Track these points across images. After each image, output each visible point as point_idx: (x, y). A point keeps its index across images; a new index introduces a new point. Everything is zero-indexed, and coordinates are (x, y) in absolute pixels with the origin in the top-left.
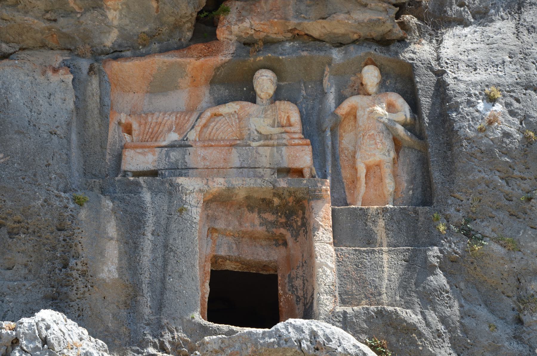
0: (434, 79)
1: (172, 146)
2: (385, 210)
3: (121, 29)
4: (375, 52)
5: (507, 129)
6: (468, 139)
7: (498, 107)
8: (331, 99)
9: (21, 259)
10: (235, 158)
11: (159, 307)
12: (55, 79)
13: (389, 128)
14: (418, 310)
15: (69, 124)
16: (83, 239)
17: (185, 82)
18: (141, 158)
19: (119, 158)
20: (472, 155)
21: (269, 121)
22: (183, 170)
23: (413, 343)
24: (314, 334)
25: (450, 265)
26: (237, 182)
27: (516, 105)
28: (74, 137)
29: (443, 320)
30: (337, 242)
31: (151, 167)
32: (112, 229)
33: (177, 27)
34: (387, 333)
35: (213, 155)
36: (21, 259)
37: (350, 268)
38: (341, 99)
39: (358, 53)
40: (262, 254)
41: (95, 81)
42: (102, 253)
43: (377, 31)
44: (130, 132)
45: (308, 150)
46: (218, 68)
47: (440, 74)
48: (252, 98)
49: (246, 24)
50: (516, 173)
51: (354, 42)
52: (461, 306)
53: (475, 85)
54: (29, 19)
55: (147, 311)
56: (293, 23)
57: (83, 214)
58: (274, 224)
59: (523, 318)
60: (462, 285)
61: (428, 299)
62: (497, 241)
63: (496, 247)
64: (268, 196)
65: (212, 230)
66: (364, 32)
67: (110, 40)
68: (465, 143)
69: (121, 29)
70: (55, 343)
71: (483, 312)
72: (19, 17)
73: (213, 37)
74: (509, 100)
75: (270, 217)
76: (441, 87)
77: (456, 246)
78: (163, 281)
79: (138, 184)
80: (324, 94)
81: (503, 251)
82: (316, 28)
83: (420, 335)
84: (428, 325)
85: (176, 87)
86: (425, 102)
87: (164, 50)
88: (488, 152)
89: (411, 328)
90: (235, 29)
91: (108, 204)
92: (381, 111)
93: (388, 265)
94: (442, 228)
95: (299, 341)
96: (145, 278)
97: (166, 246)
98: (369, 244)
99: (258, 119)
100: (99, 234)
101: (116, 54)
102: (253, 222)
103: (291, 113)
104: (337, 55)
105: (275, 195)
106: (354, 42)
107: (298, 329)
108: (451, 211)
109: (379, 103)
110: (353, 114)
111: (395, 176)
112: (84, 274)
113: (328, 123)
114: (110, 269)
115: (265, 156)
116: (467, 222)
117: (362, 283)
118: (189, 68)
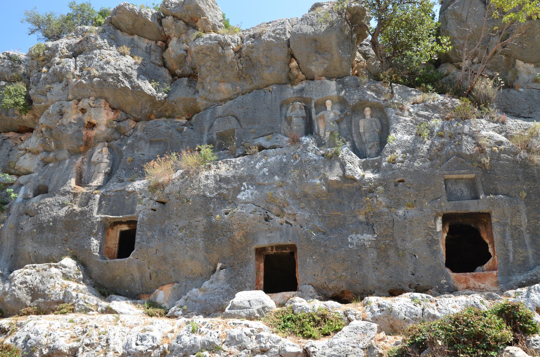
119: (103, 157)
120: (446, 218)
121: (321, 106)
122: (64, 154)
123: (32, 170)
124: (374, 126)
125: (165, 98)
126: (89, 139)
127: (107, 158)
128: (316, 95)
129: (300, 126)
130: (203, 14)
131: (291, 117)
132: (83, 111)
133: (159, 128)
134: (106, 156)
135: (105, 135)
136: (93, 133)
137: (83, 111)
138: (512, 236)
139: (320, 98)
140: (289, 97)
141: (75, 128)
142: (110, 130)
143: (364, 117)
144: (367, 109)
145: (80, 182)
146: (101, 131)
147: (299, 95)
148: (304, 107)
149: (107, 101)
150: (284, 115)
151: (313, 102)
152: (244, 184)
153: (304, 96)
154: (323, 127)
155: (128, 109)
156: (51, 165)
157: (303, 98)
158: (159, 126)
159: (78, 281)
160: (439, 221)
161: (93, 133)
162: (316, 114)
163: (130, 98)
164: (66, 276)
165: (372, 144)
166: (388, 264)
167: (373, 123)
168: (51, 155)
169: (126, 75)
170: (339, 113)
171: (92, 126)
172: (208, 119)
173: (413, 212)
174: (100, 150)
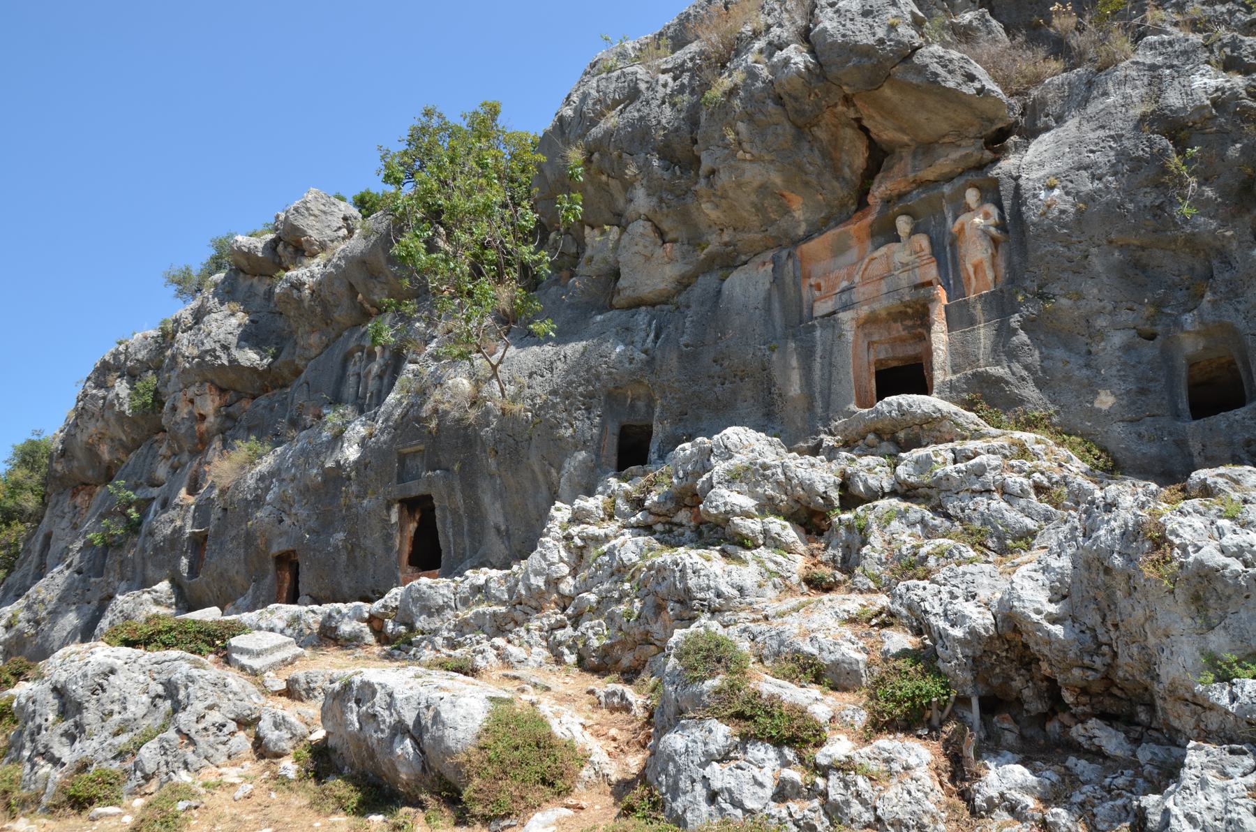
0: (1013, 183)
1: (843, 291)
2: (981, 296)
3: (806, 220)
4: (972, 177)
5: (1062, 207)
6: (1034, 224)
7: (1057, 192)
8: (950, 220)
9: (749, 394)
10: (884, 287)
11: (827, 406)
12: (761, 270)
13: (985, 232)
14: (1005, 364)
15: (768, 299)
16: (776, 373)
17: (853, 242)
18: (824, 305)
19: (812, 309)
20: (1038, 235)
21: (908, 252)
22: (846, 307)
23: (1003, 390)
24: (900, 405)
25: (1027, 325)
26: (876, 306)
27: (1070, 185)
28: (776, 305)
29: (1026, 367)
30: (950, 328)
31: (831, 310)
32: (794, 362)
33: (843, 205)
34: (981, 387)
35: (869, 289)
36: (749, 394)
37: (958, 345)
38: (956, 218)
39: (958, 182)
40: (910, 350)
41: (790, 263)
42: (789, 380)
43: (972, 162)
44: (819, 289)
45: (934, 265)
46: (871, 226)
47: (1017, 178)
48: (897, 239)
49: (883, 188)
50: (1074, 239)
51: (961, 174)
52: (1041, 353)
53: (1039, 180)
54: (752, 236)
55: (819, 410)
56: (911, 176)
57: (775, 357)
58: (913, 327)
59: (1093, 350)
60: (1042, 337)
61: (1012, 355)
62: (1065, 296)
63: (1064, 302)
64: (902, 309)
65: (870, 344)
66: (963, 165)
67: (802, 230)
68: (1032, 228)
69: (806, 220)
70: (732, 448)
71: (1059, 353)
72: (746, 236)
73: (868, 204)
74: (1065, 183)
75: (909, 323)
76: (1018, 188)
77: (1030, 310)
78: (829, 389)
79: (814, 326)
80: (945, 219)
81: (1070, 303)
82: (929, 174)
83: (1007, 383)
84: (1013, 374)
85: (850, 247)
86: (1007, 204)
87: (837, 225)
88: (1051, 229)
89: (1000, 380)
90: (877, 194)
91: (792, 345)
92: (979, 220)
93: (984, 334)
94: (1020, 298)
95: (890, 412)
96: (817, 389)
97: (830, 364)
98: (972, 325)
99: (899, 253)
100: (786, 367)
101: (808, 237)
102: (898, 329)
103: (922, 241)
104: (947, 189)
105: (906, 306)
106: (961, 174)
107: (890, 404)
108: (1028, 283)
109: (978, 215)
110: (962, 229)
111: (994, 266)
112: (780, 395)
113: (947, 241)
114: (795, 388)
115: (904, 279)
116: (1040, 287)
117: (966, 355)
118: (852, 232)
122: (185, 457)
125: (269, 365)
126: (202, 434)
130: (304, 233)
135: (216, 426)
136: (204, 426)
137: (192, 401)
138: (453, 523)
141: (188, 423)
145: (192, 491)
149: (212, 383)
155: (239, 387)
159: (169, 606)
161: (204, 426)
163: (232, 376)
164: (157, 602)
166: (356, 567)
169: (225, 348)
171: (203, 418)
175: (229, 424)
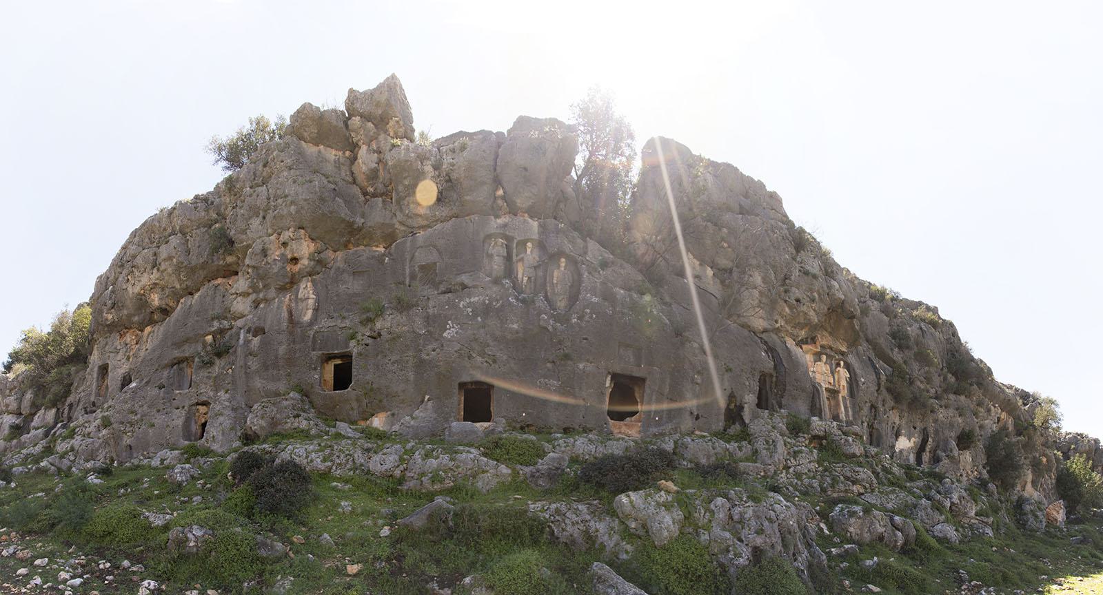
119: (309, 293)
120: (614, 377)
121: (523, 243)
123: (246, 312)
124: (566, 279)
126: (293, 275)
127: (313, 294)
128: (518, 235)
129: (501, 266)
131: (492, 255)
132: (285, 244)
133: (361, 258)
134: (311, 292)
135: (308, 270)
136: (296, 268)
139: (522, 238)
140: (492, 232)
142: (312, 263)
143: (559, 267)
144: (563, 260)
146: (304, 265)
147: (502, 232)
148: (506, 245)
150: (486, 251)
151: (515, 241)
152: (450, 322)
153: (507, 233)
154: (522, 271)
156: (262, 306)
157: (506, 234)
158: (359, 256)
160: (609, 378)
161: (296, 268)
162: (517, 256)
165: (562, 297)
167: (566, 276)
168: (261, 295)
170: (538, 259)
171: (295, 260)
172: (408, 249)
173: (590, 367)
174: (304, 286)
175: (318, 268)
